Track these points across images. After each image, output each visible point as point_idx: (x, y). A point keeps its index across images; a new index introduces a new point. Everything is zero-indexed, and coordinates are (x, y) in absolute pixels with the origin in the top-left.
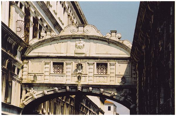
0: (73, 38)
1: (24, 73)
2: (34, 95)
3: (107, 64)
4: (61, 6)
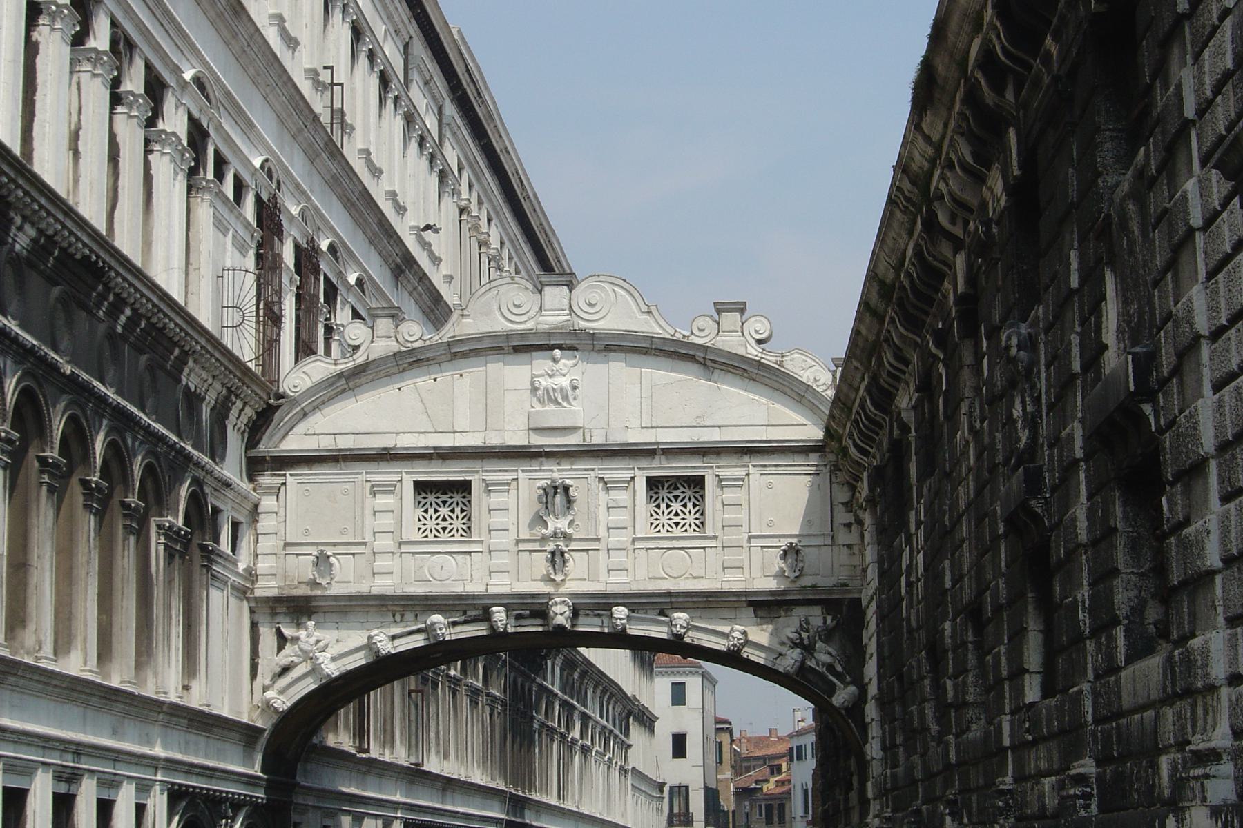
0: (517, 349)
1: (265, 544)
3: (703, 477)
4: (424, 163)
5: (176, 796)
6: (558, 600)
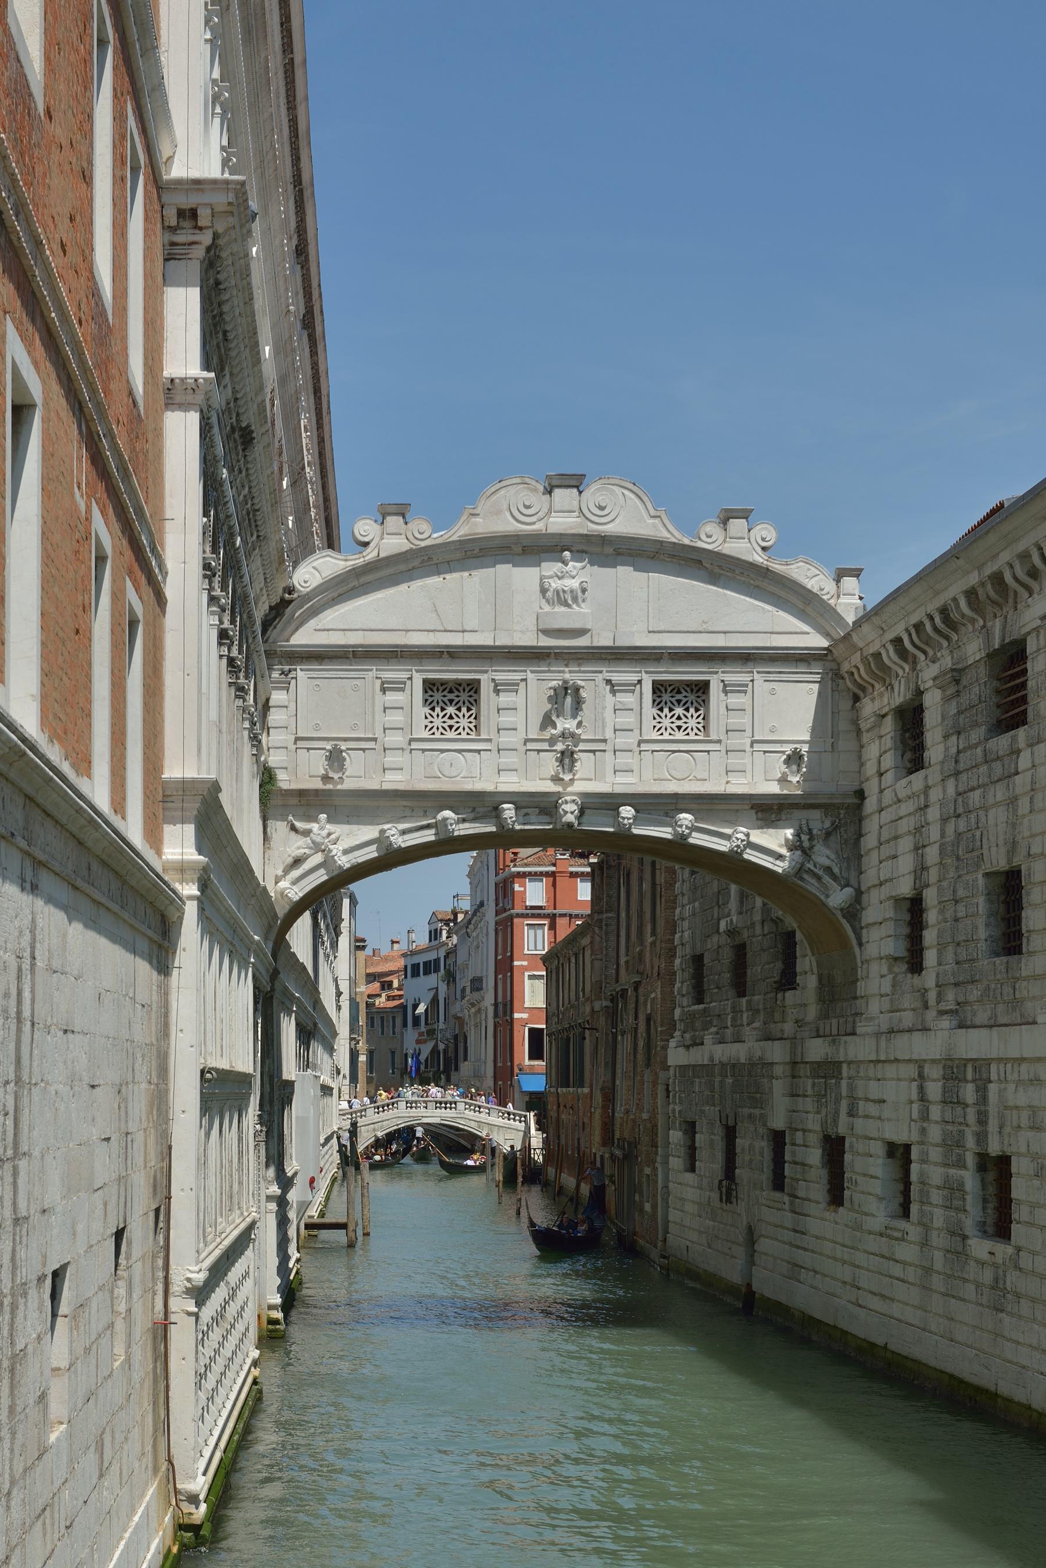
2: (336, 850)
3: (707, 683)
6: (568, 798)
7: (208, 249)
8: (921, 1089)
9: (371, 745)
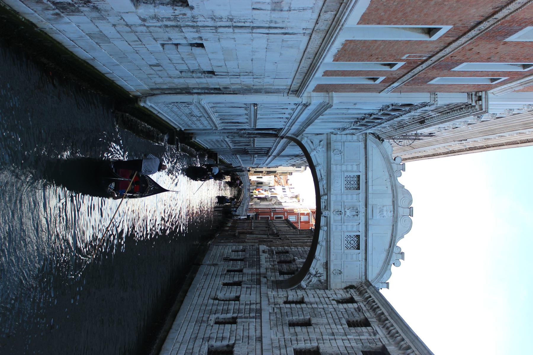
0: (393, 201)
1: (344, 137)
5: (282, 129)
7: (470, 104)
8: (254, 303)
9: (343, 162)
